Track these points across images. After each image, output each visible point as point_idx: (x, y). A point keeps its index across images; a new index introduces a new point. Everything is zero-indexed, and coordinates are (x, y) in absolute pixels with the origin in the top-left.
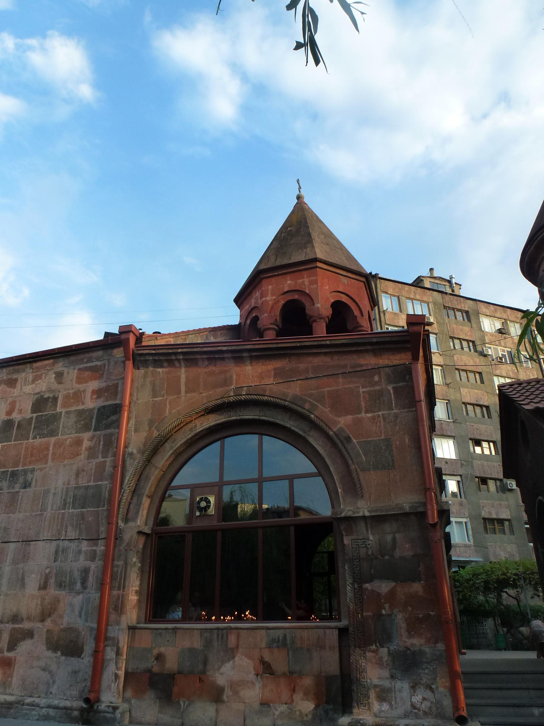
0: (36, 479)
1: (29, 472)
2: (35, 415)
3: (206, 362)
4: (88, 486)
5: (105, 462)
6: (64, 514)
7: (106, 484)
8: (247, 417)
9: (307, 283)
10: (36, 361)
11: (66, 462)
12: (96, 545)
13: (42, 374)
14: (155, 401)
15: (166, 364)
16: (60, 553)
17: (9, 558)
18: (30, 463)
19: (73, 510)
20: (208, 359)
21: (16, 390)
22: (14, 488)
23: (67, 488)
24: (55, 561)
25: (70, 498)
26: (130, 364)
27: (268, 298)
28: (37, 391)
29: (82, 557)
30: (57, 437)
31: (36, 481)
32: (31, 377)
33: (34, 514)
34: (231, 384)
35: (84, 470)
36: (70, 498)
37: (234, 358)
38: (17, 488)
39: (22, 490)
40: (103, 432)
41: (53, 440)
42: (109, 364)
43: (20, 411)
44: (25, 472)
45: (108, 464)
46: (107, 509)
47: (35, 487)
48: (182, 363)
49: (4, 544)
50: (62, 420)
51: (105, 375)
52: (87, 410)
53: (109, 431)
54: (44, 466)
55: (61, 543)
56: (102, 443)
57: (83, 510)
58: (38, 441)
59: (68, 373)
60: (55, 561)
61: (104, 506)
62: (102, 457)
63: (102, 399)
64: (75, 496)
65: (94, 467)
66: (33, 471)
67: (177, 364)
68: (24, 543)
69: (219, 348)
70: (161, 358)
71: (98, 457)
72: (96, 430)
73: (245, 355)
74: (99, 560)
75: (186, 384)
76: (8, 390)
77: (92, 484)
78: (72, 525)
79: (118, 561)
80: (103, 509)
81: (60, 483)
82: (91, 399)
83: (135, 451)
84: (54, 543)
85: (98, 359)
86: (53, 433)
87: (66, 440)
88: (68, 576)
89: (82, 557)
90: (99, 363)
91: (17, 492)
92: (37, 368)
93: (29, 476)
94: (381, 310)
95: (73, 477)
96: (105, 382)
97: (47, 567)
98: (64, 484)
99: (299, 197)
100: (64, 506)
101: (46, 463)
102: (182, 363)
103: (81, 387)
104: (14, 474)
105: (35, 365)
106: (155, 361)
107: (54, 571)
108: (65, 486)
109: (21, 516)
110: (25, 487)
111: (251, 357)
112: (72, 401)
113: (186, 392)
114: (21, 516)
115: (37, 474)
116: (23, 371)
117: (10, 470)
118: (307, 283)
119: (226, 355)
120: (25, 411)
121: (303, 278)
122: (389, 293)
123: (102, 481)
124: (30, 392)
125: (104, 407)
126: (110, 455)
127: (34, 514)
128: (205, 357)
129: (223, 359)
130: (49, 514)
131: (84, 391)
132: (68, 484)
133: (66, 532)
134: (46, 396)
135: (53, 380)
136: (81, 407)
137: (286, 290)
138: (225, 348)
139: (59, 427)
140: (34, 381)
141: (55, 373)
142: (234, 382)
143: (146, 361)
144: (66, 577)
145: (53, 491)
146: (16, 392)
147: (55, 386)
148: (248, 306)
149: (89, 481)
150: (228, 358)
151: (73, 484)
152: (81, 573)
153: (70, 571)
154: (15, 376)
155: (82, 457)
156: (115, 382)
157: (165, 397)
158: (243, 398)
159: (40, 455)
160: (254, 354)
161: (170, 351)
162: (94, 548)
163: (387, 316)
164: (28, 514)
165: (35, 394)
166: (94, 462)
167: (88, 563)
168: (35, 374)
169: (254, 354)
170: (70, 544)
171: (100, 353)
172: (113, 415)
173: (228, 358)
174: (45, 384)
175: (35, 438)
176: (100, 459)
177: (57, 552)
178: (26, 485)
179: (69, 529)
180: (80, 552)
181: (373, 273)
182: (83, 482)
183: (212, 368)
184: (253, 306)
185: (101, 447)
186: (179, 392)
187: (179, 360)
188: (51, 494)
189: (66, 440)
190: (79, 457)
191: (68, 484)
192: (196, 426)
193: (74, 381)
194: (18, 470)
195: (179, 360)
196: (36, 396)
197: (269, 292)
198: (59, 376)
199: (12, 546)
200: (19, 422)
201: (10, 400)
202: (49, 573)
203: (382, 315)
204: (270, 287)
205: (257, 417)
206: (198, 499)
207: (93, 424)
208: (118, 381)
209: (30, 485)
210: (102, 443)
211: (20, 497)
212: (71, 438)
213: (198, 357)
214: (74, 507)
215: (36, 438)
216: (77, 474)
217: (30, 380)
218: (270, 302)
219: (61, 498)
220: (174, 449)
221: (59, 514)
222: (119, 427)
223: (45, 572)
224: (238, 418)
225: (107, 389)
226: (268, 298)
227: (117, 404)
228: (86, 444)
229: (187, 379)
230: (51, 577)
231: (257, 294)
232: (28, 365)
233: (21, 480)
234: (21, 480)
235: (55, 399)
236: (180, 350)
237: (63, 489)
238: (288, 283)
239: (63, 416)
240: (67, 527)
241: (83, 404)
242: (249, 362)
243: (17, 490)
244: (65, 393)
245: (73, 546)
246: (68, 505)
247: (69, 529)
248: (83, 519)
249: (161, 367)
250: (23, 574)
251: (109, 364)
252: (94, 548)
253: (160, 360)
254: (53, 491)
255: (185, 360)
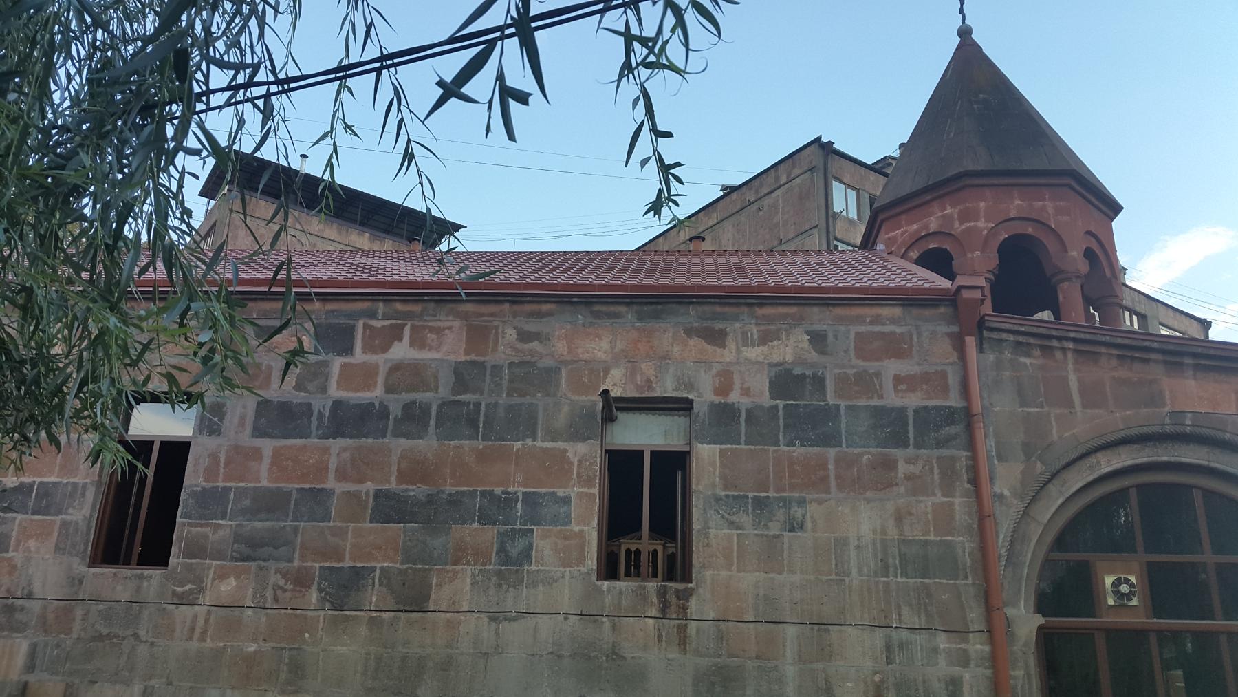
0: (812, 517)
1: (794, 504)
2: (781, 403)
3: (1114, 362)
4: (926, 542)
5: (952, 504)
6: (887, 584)
7: (963, 542)
8: (1188, 460)
9: (1051, 211)
10: (761, 305)
11: (869, 494)
12: (966, 641)
13: (779, 330)
14: (1029, 413)
15: (1037, 352)
16: (897, 650)
17: (790, 652)
18: (793, 487)
19: (904, 580)
20: (1119, 356)
21: (726, 351)
22: (768, 528)
23: (883, 541)
24: (888, 663)
25: (894, 558)
26: (971, 342)
27: (981, 224)
28: (776, 358)
29: (942, 662)
30: (838, 449)
31: (814, 521)
32: (754, 331)
33: (824, 578)
34: (1164, 405)
35: (911, 514)
36: (894, 558)
37: (1165, 362)
38: (774, 529)
39: (785, 533)
40: (936, 453)
41: (832, 452)
42: (919, 335)
43: (746, 392)
44: (786, 503)
45: (957, 508)
46: (974, 584)
47: (814, 530)
48: (1070, 355)
49: (773, 626)
50: (843, 420)
51: (914, 352)
52: (893, 409)
53: (945, 452)
54: (824, 496)
55: (894, 633)
56: (936, 471)
57: (927, 581)
58: (799, 451)
59: (836, 337)
60: (888, 663)
61: (966, 578)
62: (944, 495)
63: (919, 394)
64: (903, 557)
65: (929, 509)
66: (802, 502)
67: (1059, 354)
68: (816, 627)
69: (1147, 344)
70: (1032, 340)
71: (934, 494)
72: (918, 446)
73: (1188, 360)
74: (977, 666)
75: (1082, 392)
76: (710, 348)
77: (932, 538)
78: (910, 605)
79: (1014, 669)
80: (968, 584)
81: (866, 529)
82: (896, 391)
83: (1006, 493)
84: (879, 635)
85: (894, 321)
86: (829, 440)
87: (861, 455)
88: (921, 688)
89: (942, 662)
90: (898, 330)
91: (777, 537)
92: (769, 319)
93: (798, 513)
94: (830, 213)
95: (891, 523)
96: (919, 365)
97: (876, 673)
98: (874, 532)
99: (965, 32)
100: (885, 569)
101: (828, 491)
102: (1070, 355)
103: (872, 366)
104: (760, 503)
105: (760, 311)
106: (1019, 343)
107: (891, 680)
108: (878, 537)
109: (797, 578)
110: (792, 530)
111: (1197, 367)
112: (856, 388)
113: (1084, 406)
114: (797, 578)
115: (812, 509)
116: (736, 318)
117: (751, 495)
118: (1051, 211)
119: (1153, 356)
120: (753, 390)
121: (1044, 200)
122: (845, 180)
123: (952, 535)
124: (761, 359)
125: (925, 408)
126: (958, 494)
127: (824, 578)
128: (1115, 352)
129: (1146, 361)
130: (856, 583)
131: (878, 374)
132: (884, 532)
133: (900, 615)
134: (797, 371)
135: (806, 345)
136: (875, 402)
137: (1012, 215)
138: (1155, 345)
139: (839, 433)
140: (764, 339)
141: (808, 333)
142: (1168, 402)
143: (1000, 341)
144: (917, 690)
145: (853, 542)
146: (728, 355)
147: (813, 356)
148: (915, 227)
149: (927, 533)
150: (1156, 361)
151: (893, 534)
152: (947, 685)
153: (924, 682)
154: (719, 325)
155: (902, 489)
156: (939, 369)
157: (1046, 409)
158: (1188, 429)
159: (815, 479)
160: (1203, 362)
161: (1054, 333)
162: (962, 646)
163: (839, 225)
164: (812, 577)
165: (771, 365)
166: (927, 504)
167: (956, 670)
168: (763, 328)
169: (1203, 362)
170: (914, 636)
171: (897, 311)
172: (948, 425)
173: (1156, 361)
174: (789, 350)
175: (790, 443)
176: (939, 498)
177: (888, 648)
178: (794, 526)
179: (905, 611)
180: (935, 650)
181: (824, 140)
182: (914, 532)
183: (1123, 373)
184: (933, 227)
185: (936, 477)
186: (1070, 404)
187: (1064, 349)
188: (852, 548)
189: (861, 455)
190: (895, 488)
191: (884, 532)
192: (1099, 463)
193: (852, 353)
194: (768, 497)
195: (1064, 349)
196: (774, 370)
197: (982, 214)
198: (818, 340)
199: (791, 631)
200: (749, 412)
201: (716, 368)
202: (882, 681)
203: (831, 220)
204: (982, 204)
205: (1205, 463)
206: (1109, 581)
207: (911, 435)
208: (946, 368)
209: (801, 527)
210: (936, 471)
211: (786, 546)
212: (869, 453)
213: (1103, 350)
214: (904, 574)
215: (795, 445)
216: (899, 518)
217: (755, 337)
218: (985, 232)
219: (875, 555)
220: (1067, 495)
221: (877, 583)
222: (971, 445)
223: (873, 681)
224: (1172, 459)
225: (925, 378)
226: (981, 224)
227: (949, 407)
228: (902, 469)
229: (1080, 380)
230: (887, 688)
231: (949, 211)
232: (746, 309)
233: (780, 515)
234: (780, 515)
235: (819, 382)
236: (1072, 335)
237: (874, 543)
238: (1016, 205)
239: (842, 412)
240: (899, 607)
241: (882, 397)
242: (1191, 373)
243: (774, 529)
244: (837, 371)
245: (919, 639)
246: (891, 570)
247: (905, 611)
248: (929, 595)
249: (1028, 355)
250: (826, 681)
251: (919, 335)
252: (962, 646)
253: (1028, 344)
254: (853, 542)
255: (1075, 351)
